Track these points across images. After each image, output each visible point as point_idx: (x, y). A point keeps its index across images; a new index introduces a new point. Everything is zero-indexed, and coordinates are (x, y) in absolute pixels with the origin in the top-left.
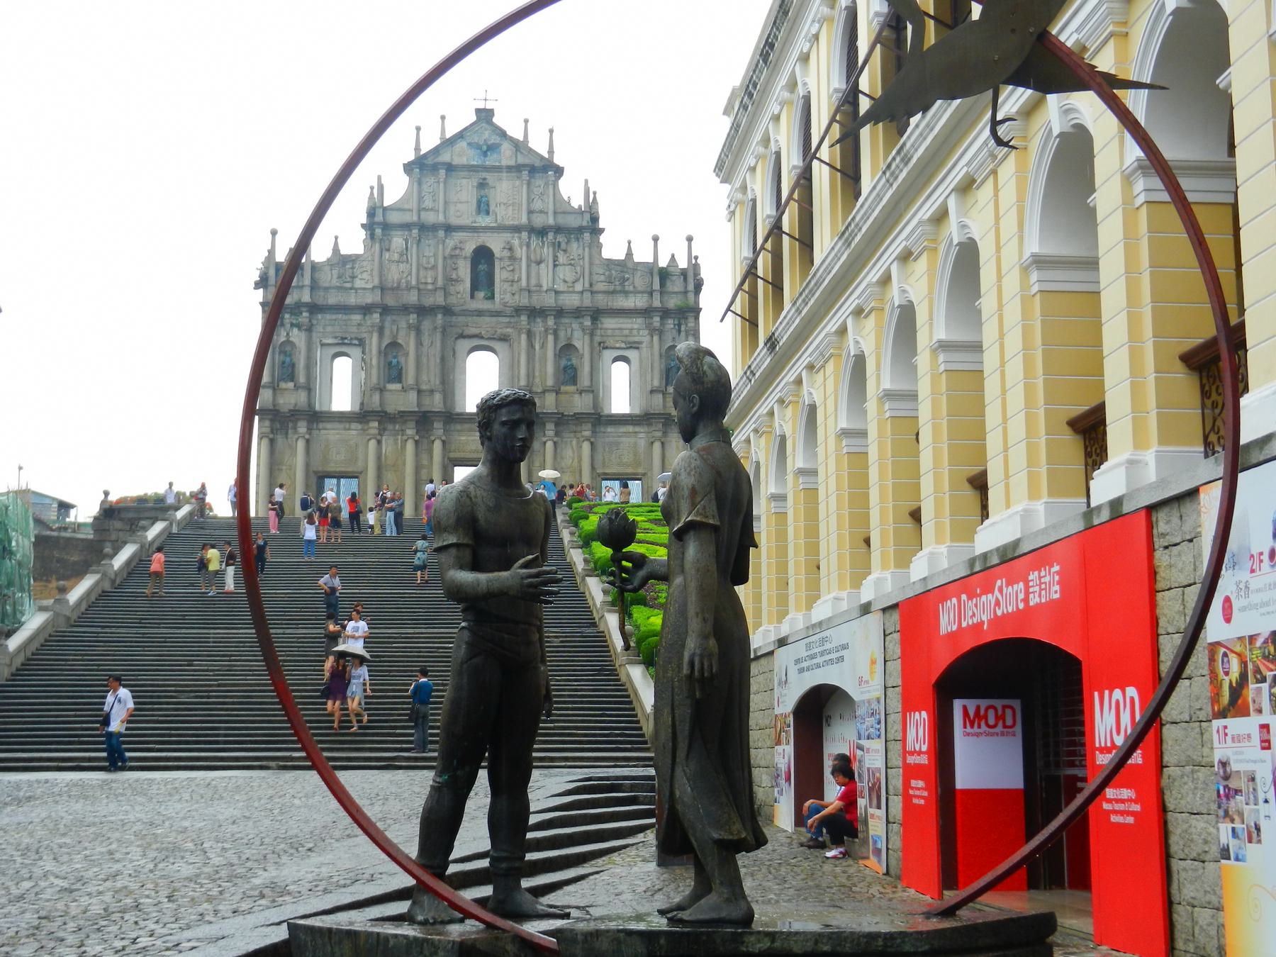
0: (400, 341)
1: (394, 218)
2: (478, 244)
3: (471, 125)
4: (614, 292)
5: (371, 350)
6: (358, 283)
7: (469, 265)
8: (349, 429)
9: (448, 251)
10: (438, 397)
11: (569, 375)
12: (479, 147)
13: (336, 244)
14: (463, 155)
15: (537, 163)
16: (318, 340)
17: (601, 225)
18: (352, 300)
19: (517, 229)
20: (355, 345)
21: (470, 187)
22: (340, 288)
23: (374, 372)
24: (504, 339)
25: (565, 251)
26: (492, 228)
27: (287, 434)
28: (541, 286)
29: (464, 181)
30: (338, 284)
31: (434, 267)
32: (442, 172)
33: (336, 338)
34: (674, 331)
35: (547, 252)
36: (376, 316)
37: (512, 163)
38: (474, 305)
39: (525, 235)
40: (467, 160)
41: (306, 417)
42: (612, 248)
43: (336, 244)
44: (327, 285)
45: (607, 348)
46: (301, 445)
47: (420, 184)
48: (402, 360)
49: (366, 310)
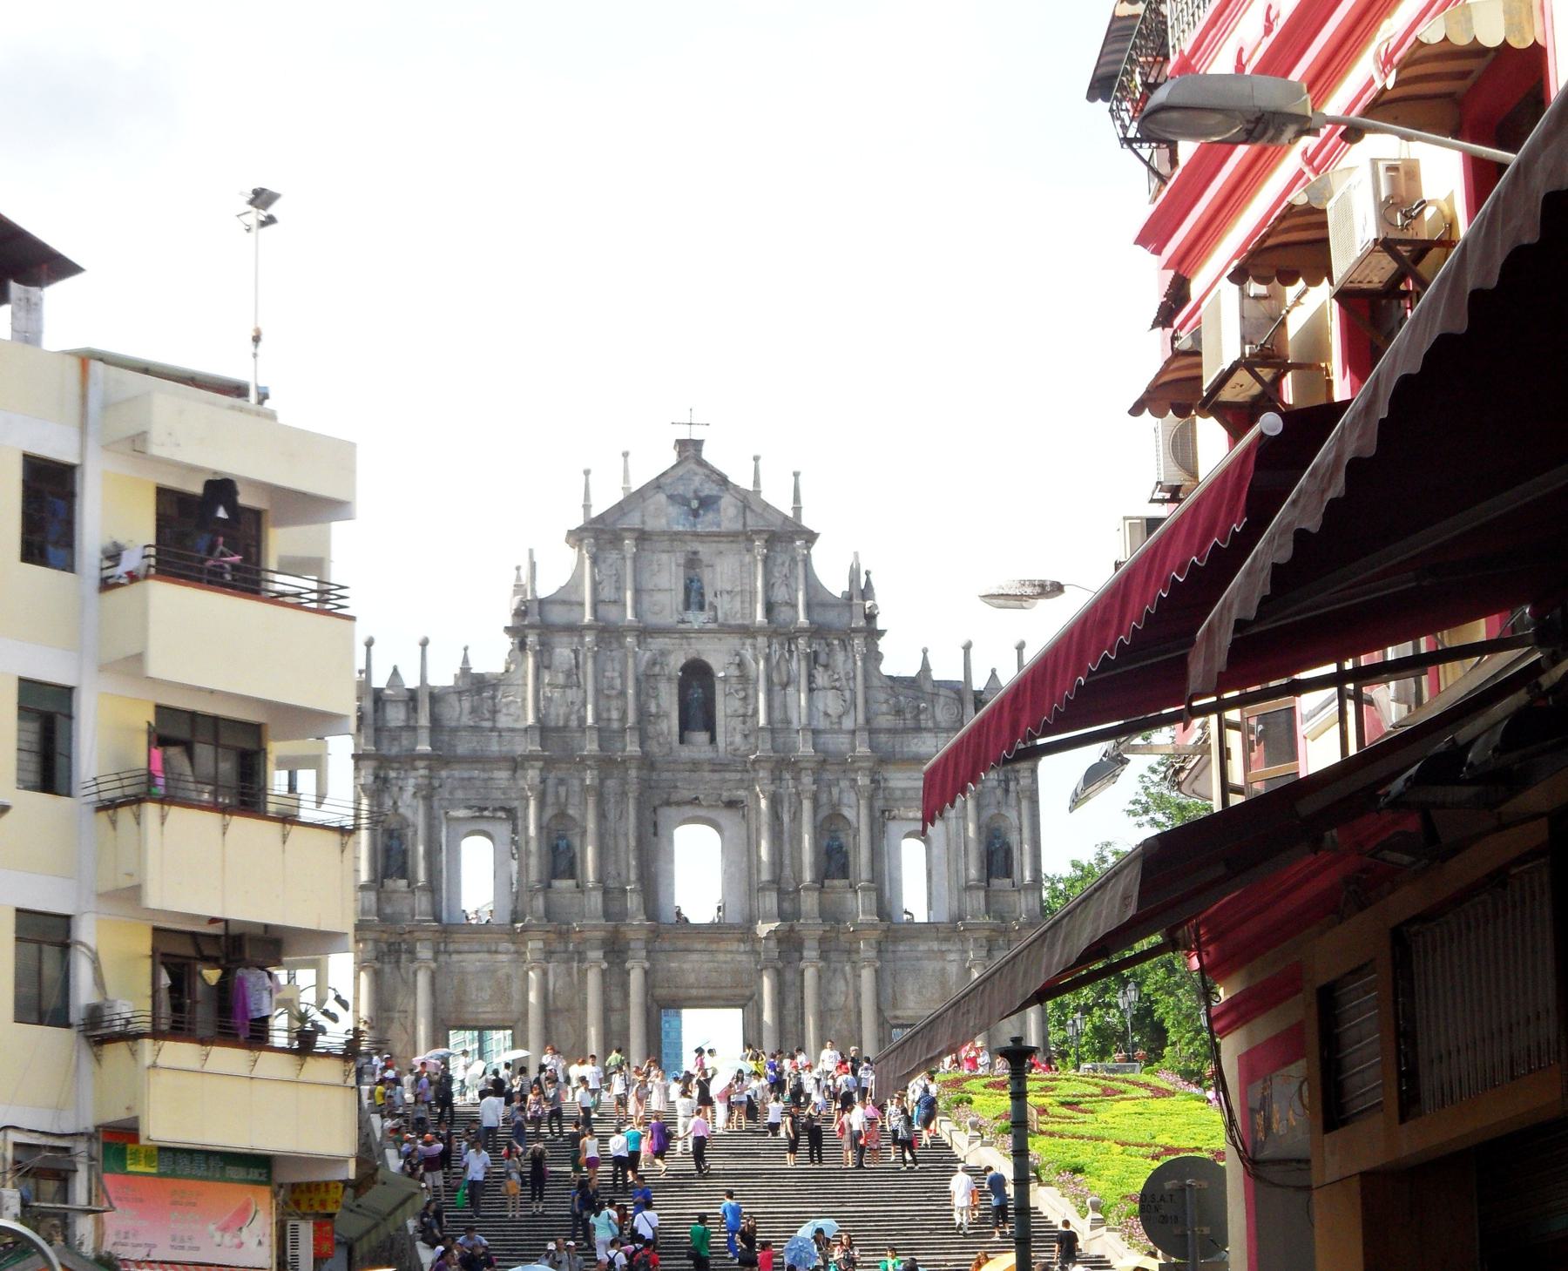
0: (571, 812)
1: (557, 615)
2: (690, 657)
3: (673, 468)
4: (905, 731)
5: (527, 828)
6: (503, 721)
7: (675, 691)
8: (496, 952)
9: (642, 668)
11: (834, 862)
12: (685, 502)
13: (466, 660)
14: (664, 516)
15: (777, 526)
16: (442, 812)
17: (880, 624)
18: (494, 748)
20: (500, 818)
21: (674, 568)
22: (475, 729)
23: (533, 862)
24: (732, 804)
25: (826, 667)
26: (710, 631)
27: (398, 962)
28: (788, 722)
29: (665, 557)
30: (472, 724)
31: (622, 694)
32: (629, 544)
33: (470, 808)
34: (999, 792)
35: (798, 667)
37: (738, 526)
38: (685, 753)
39: (761, 641)
40: (668, 524)
41: (430, 935)
42: (898, 661)
43: (466, 660)
44: (453, 724)
45: (894, 818)
46: (422, 980)
47: (595, 561)
48: (576, 842)
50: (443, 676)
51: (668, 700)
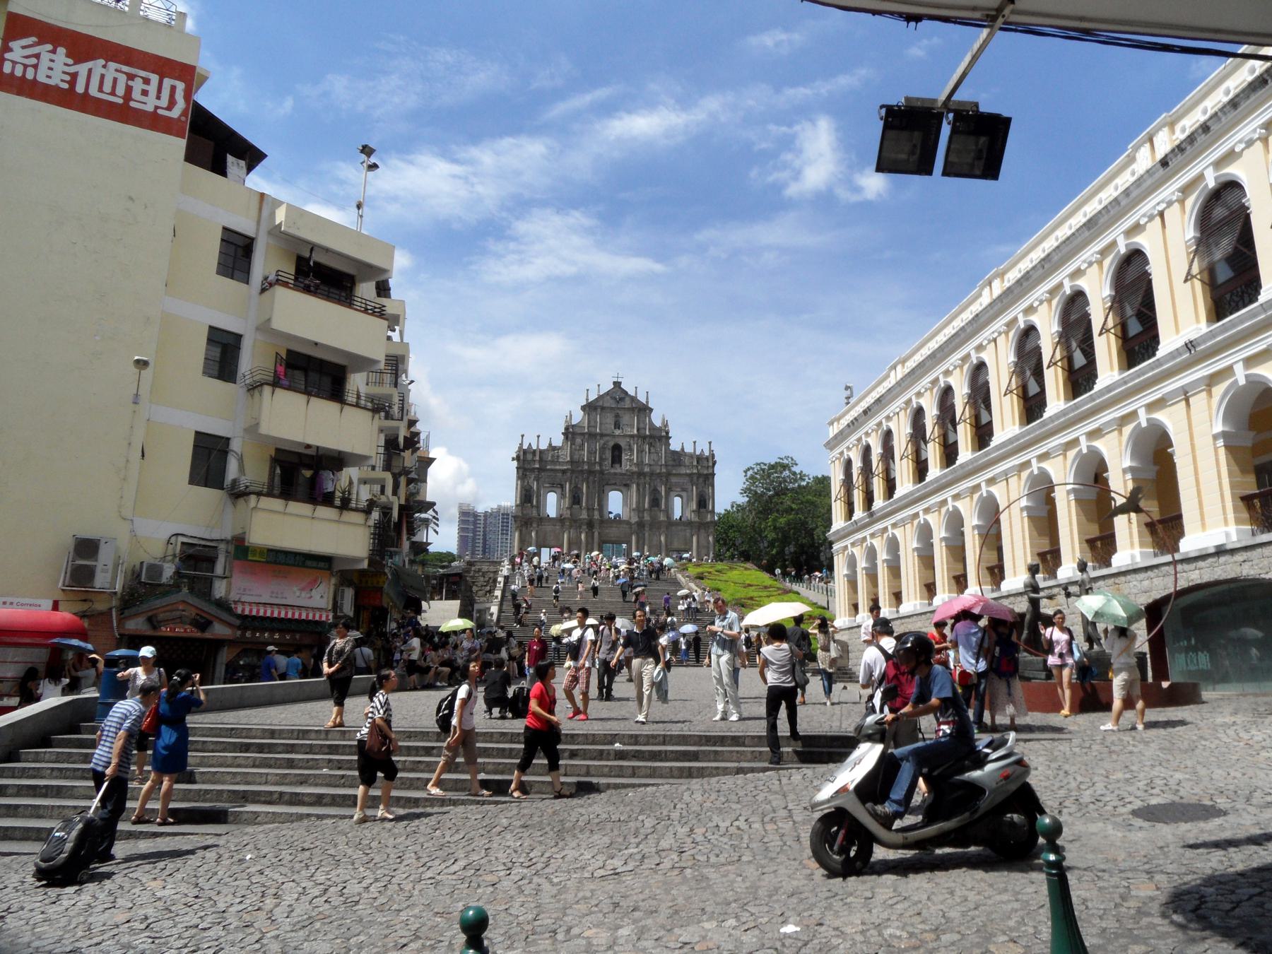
10: (596, 513)
11: (655, 502)
14: (609, 403)
19: (632, 436)
24: (626, 485)
36: (569, 474)
38: (612, 471)
42: (675, 445)
49: (564, 472)
50: (544, 446)
51: (608, 455)
